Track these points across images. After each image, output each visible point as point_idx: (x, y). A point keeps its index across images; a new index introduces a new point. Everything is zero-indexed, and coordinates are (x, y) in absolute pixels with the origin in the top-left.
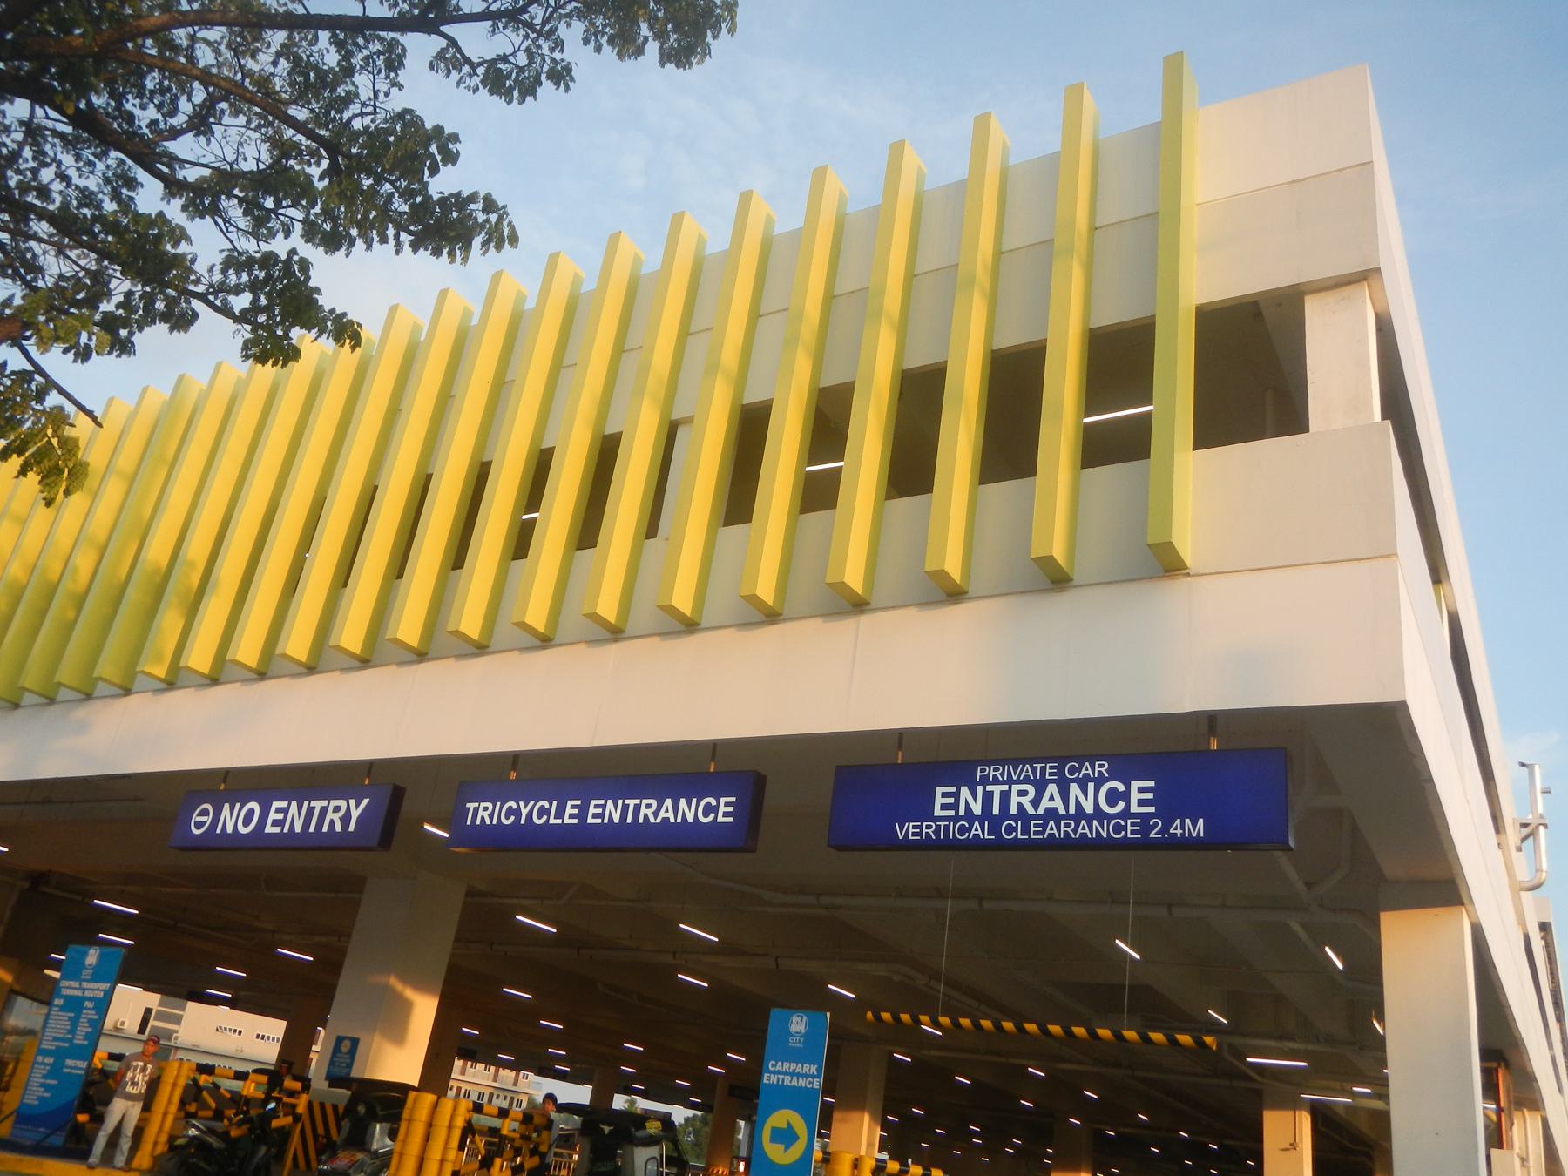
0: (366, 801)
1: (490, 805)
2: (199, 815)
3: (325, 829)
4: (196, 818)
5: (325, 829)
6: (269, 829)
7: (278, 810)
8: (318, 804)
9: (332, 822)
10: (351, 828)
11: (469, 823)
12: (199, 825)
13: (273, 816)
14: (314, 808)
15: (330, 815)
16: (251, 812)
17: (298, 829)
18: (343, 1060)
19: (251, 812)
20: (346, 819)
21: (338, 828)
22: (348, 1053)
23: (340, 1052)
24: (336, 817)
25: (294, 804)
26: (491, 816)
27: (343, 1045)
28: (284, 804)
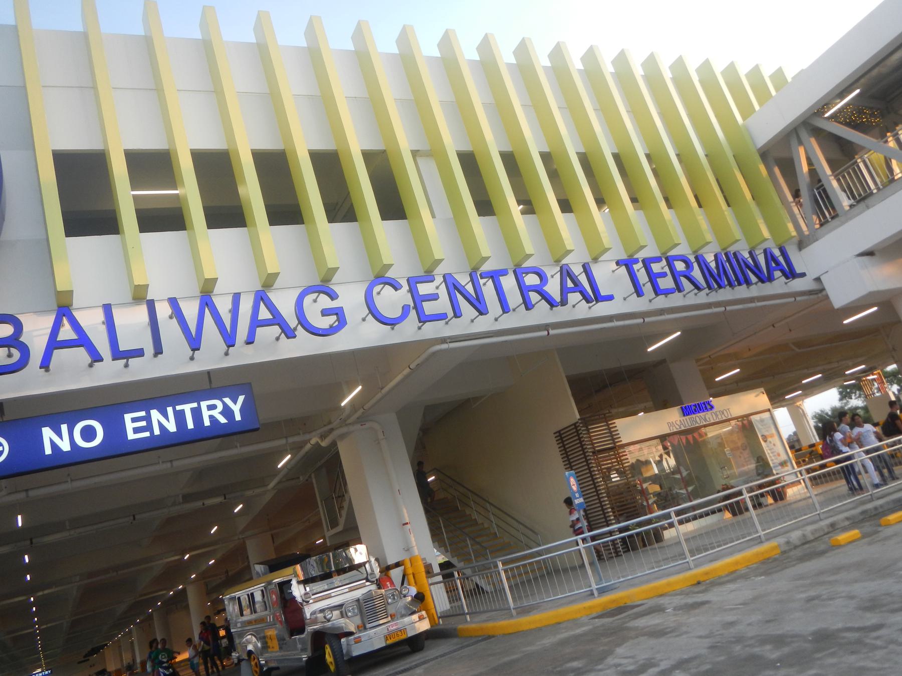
0: (241, 399)
7: (134, 420)
9: (211, 417)
10: (238, 417)
14: (183, 411)
20: (227, 412)
21: (223, 420)
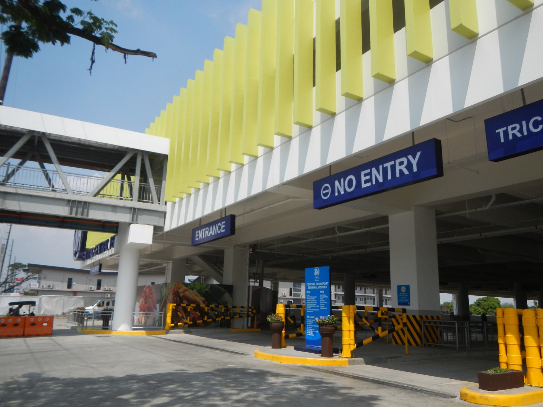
0: (418, 154)
1: (517, 126)
2: (324, 190)
3: (398, 175)
4: (322, 192)
5: (398, 175)
6: (364, 186)
7: (365, 175)
8: (388, 165)
9: (401, 171)
10: (415, 170)
11: (502, 140)
12: (325, 195)
13: (363, 179)
14: (387, 167)
15: (398, 168)
16: (350, 181)
17: (381, 180)
18: (404, 296)
19: (350, 181)
20: (409, 166)
21: (406, 172)
22: (405, 292)
23: (402, 292)
24: (403, 167)
25: (374, 170)
26: (521, 131)
27: (402, 289)
28: (368, 171)
